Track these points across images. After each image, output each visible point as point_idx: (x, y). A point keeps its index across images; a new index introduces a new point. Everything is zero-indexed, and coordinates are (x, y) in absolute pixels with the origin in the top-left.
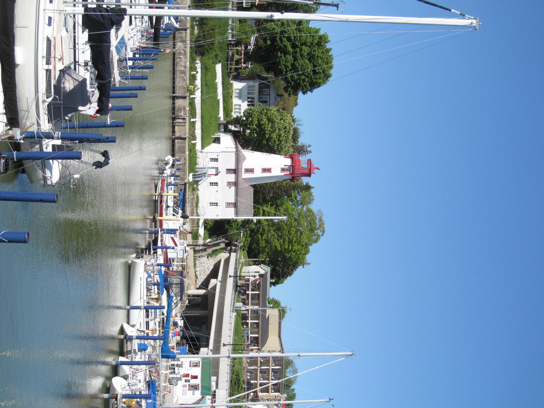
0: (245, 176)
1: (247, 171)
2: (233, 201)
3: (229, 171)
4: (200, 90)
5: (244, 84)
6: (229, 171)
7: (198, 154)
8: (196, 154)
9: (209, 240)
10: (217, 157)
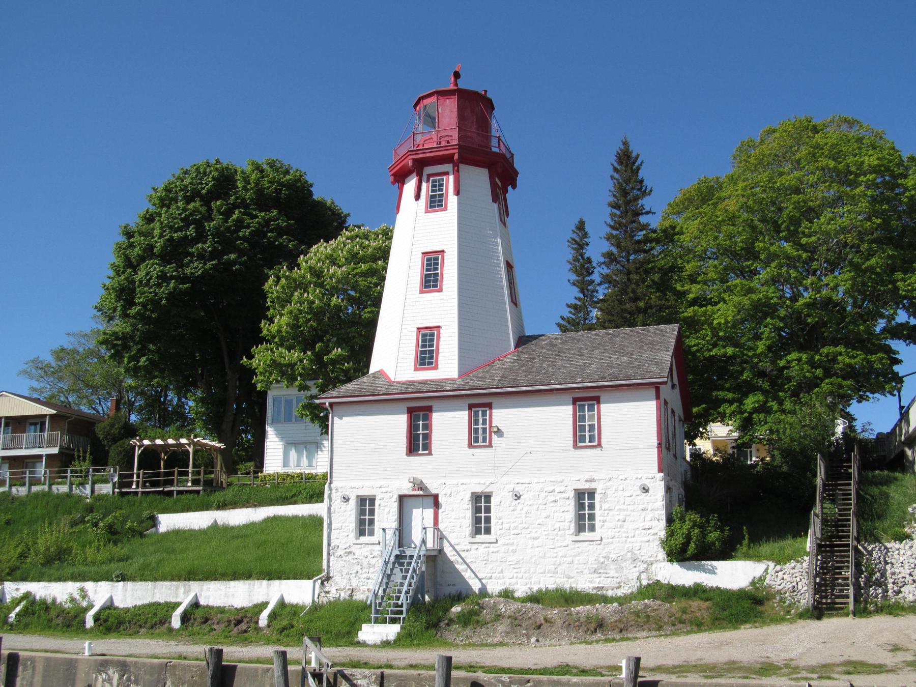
0: (448, 366)
2: (563, 414)
3: (418, 442)
4: (89, 586)
5: (270, 431)
6: (418, 442)
7: (333, 594)
8: (335, 605)
10: (353, 503)
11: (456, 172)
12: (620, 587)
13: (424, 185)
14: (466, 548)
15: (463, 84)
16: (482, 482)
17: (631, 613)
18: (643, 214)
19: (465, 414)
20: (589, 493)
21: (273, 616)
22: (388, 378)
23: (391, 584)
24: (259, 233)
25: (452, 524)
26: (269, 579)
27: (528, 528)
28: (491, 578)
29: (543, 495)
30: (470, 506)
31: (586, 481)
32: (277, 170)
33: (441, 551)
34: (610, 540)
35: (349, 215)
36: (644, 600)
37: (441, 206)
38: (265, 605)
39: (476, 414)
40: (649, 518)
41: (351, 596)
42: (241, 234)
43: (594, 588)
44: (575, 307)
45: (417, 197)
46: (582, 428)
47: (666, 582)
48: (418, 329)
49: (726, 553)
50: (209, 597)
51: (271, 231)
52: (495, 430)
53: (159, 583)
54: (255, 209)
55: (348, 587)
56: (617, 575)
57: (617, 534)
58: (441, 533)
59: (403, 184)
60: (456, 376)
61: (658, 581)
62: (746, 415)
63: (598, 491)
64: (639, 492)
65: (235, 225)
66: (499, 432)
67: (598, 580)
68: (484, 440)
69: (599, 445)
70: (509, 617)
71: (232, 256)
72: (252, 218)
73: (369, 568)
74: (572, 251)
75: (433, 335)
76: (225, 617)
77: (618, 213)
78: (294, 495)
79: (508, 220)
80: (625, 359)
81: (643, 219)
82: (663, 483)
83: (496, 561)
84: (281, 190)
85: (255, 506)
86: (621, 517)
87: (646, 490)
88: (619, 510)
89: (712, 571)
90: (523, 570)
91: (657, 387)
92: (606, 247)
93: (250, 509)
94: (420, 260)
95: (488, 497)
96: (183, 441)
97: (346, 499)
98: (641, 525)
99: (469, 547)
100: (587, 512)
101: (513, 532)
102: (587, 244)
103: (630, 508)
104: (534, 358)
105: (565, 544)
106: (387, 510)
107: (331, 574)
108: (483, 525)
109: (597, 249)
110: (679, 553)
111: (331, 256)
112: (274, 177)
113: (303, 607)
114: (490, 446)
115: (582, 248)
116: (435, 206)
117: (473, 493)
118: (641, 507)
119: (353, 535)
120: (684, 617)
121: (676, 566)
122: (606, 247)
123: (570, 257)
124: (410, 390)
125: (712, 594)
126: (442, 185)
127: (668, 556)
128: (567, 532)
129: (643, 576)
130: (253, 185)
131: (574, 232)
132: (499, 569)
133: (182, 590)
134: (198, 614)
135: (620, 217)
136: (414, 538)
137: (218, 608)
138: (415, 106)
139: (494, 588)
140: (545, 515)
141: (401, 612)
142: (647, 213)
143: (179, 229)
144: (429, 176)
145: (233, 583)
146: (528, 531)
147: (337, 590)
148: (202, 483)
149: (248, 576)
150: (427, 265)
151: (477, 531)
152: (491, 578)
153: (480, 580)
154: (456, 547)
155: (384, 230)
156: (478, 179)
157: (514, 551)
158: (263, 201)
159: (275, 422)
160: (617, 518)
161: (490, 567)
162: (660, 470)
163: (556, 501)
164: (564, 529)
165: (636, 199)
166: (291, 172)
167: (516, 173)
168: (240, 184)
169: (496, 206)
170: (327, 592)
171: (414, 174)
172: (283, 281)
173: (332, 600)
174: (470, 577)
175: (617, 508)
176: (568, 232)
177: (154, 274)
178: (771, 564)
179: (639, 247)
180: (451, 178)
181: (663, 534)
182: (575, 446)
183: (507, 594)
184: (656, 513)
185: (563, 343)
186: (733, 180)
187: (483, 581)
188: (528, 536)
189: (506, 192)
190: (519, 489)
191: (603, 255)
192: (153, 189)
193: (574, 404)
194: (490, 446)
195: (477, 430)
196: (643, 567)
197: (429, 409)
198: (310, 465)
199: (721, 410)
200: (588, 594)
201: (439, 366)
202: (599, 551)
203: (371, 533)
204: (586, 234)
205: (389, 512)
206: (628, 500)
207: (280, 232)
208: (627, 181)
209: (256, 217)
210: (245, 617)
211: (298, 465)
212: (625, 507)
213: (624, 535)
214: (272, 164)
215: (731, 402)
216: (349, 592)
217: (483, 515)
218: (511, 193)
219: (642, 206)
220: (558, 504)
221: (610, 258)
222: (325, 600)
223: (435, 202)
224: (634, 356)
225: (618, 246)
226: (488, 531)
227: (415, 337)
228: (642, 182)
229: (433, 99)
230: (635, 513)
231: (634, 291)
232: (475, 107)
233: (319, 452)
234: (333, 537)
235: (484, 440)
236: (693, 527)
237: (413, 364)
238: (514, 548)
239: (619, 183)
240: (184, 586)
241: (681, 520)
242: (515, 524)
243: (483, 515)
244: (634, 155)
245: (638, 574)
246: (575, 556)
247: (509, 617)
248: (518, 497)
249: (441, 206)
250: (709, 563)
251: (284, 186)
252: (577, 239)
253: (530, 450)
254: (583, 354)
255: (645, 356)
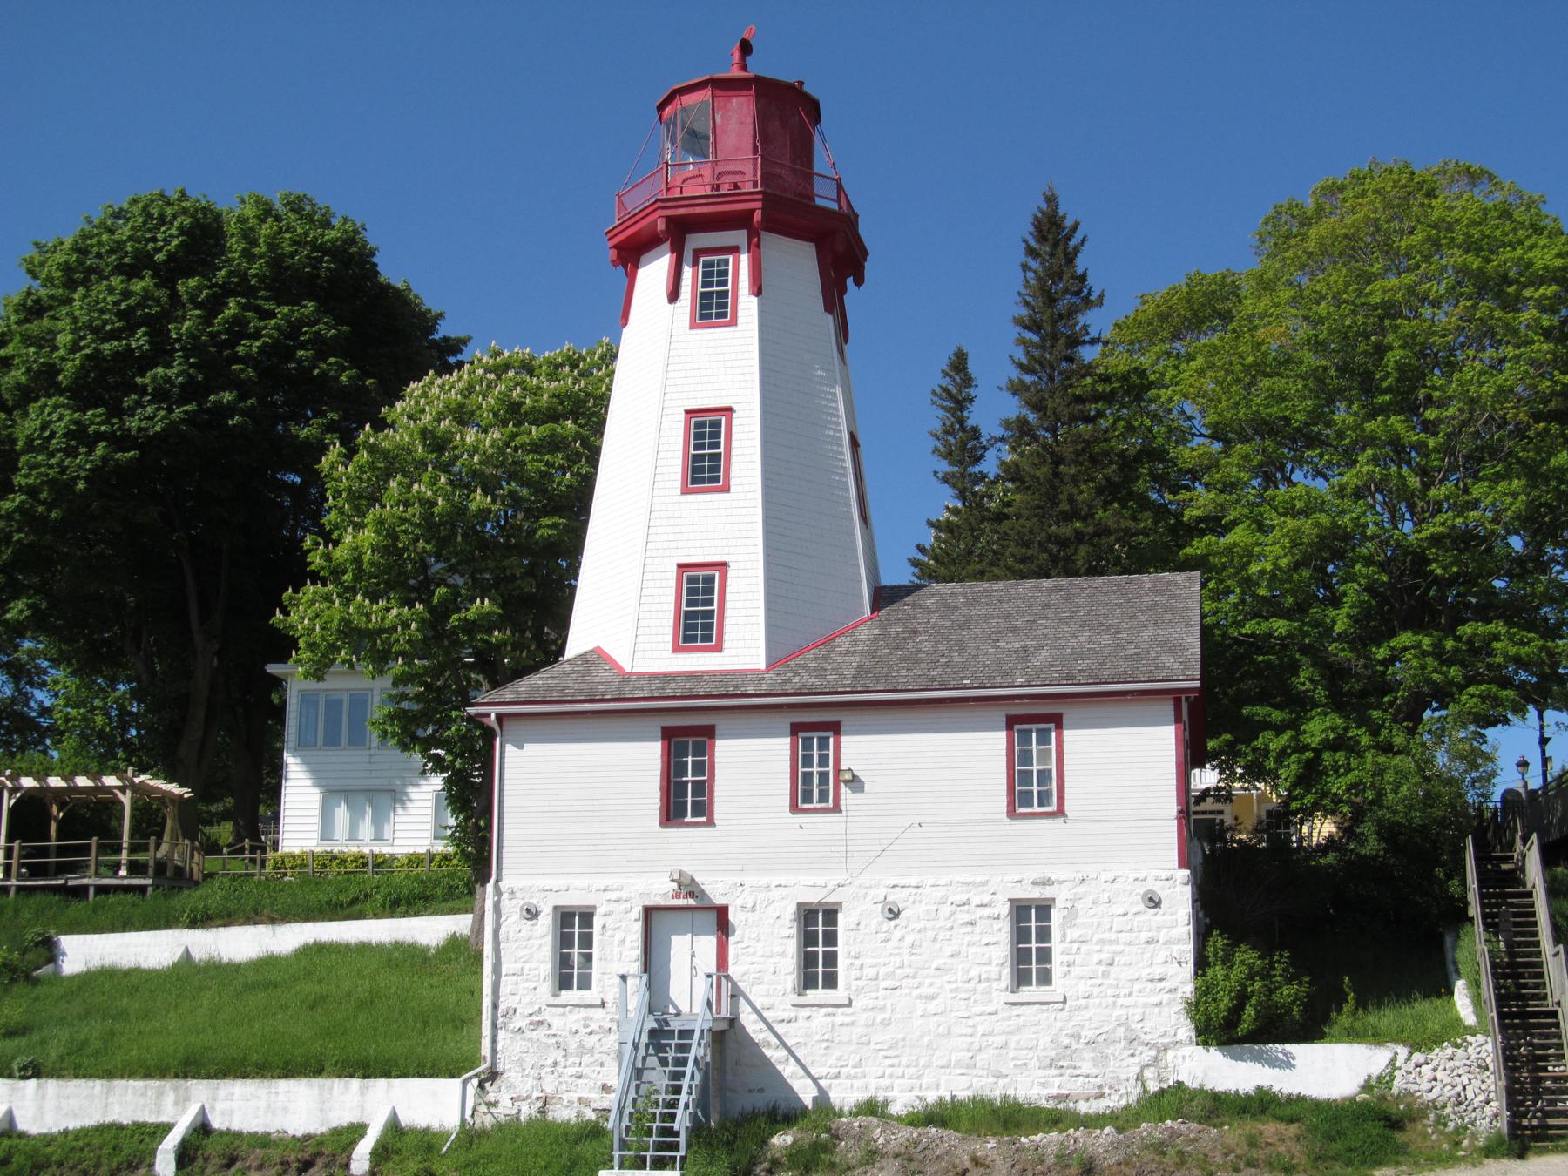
0: (744, 645)
1: (698, 619)
3: (684, 799)
5: (294, 766)
6: (684, 799)
7: (505, 1108)
8: (509, 1130)
9: (1462, 1002)
10: (546, 922)
11: (754, 247)
12: (1102, 1095)
13: (687, 272)
14: (786, 1015)
15: (758, 66)
16: (821, 881)
17: (1146, 1147)
18: (1084, 342)
19: (784, 743)
20: (1038, 908)
21: (381, 1153)
22: (615, 664)
23: (644, 1089)
24: (280, 351)
25: (758, 968)
26: (365, 1077)
27: (914, 977)
28: (837, 1076)
29: (946, 910)
30: (794, 931)
31: (1034, 883)
32: (310, 218)
33: (733, 1021)
34: (1083, 1002)
35: (441, 316)
36: (1162, 1120)
37: (724, 315)
38: (358, 1130)
39: (807, 744)
40: (1160, 958)
41: (543, 1111)
42: (241, 350)
43: (1049, 1098)
44: (948, 527)
45: (673, 296)
46: (1026, 777)
47: (1195, 1085)
48: (680, 566)
49: (1311, 1031)
50: (231, 1112)
51: (303, 346)
52: (848, 776)
53: (119, 1084)
54: (267, 299)
55: (536, 1094)
56: (1095, 1071)
57: (1096, 991)
58: (734, 984)
59: (636, 266)
60: (763, 666)
61: (1180, 1083)
62: (1309, 754)
63: (1059, 904)
64: (1141, 907)
65: (227, 331)
66: (855, 783)
67: (1057, 1081)
68: (823, 796)
69: (1061, 812)
70: (896, 1156)
71: (227, 397)
72: (262, 319)
73: (581, 1055)
74: (941, 413)
75: (711, 579)
76: (275, 1154)
77: (1035, 338)
78: (354, 901)
79: (846, 347)
80: (1106, 639)
81: (1088, 354)
82: (1189, 888)
83: (849, 1042)
84: (320, 260)
85: (272, 921)
86: (1105, 956)
87: (1154, 902)
88: (1102, 941)
89: (1287, 1063)
90: (904, 1060)
91: (1176, 696)
92: (1013, 408)
93: (261, 928)
94: (682, 425)
95: (831, 914)
96: (110, 781)
97: (532, 914)
98: (1145, 973)
99: (793, 1015)
100: (1034, 945)
101: (883, 984)
102: (972, 400)
103: (1123, 937)
104: (916, 632)
105: (991, 1009)
106: (619, 936)
107: (500, 1068)
108: (820, 969)
109: (994, 409)
110: (1221, 1027)
111: (461, 406)
112: (306, 234)
113: (444, 1135)
114: (836, 809)
115: (961, 408)
116: (710, 316)
117: (799, 905)
118: (1144, 936)
119: (546, 987)
120: (1254, 1153)
121: (1215, 1056)
122: (1013, 408)
123: (937, 426)
124: (669, 692)
125: (1295, 1108)
126: (726, 273)
127: (1199, 1033)
128: (995, 985)
129: (1149, 1074)
130: (264, 249)
131: (946, 374)
132: (854, 1059)
133: (170, 1098)
134: (213, 1148)
135: (1042, 347)
136: (673, 994)
137: (254, 1135)
138: (661, 107)
139: (845, 1096)
140: (949, 951)
141: (676, 1147)
142: (1093, 342)
143: (114, 335)
144: (697, 253)
145: (283, 1085)
146: (916, 982)
147: (512, 1099)
148: (151, 871)
149: (315, 1069)
150: (697, 436)
151: (808, 982)
152: (837, 1076)
153: (815, 1080)
154: (766, 1014)
155: (569, 358)
156: (797, 261)
157: (886, 1023)
158: (286, 281)
159: (302, 746)
160: (1096, 957)
161: (837, 1054)
162: (1182, 865)
163: (972, 924)
164: (988, 980)
165: (1072, 312)
166: (336, 222)
167: (865, 253)
168: (235, 245)
169: (830, 318)
170: (494, 1104)
171: (667, 245)
172: (364, 456)
173: (502, 1119)
174: (793, 1075)
175: (1096, 937)
176: (935, 377)
177: (60, 427)
178: (1402, 1051)
179: (1080, 408)
180: (744, 259)
181: (1188, 989)
182: (1012, 813)
183: (872, 1108)
184: (1175, 948)
185: (968, 603)
186: (1266, 285)
187: (822, 1082)
188: (915, 993)
189: (843, 290)
190: (896, 897)
191: (1007, 424)
192: (37, 245)
193: (1009, 727)
194: (836, 809)
195: (808, 777)
196: (1148, 1055)
197: (709, 732)
198: (378, 837)
199: (1259, 743)
200: (1039, 1111)
201: (726, 645)
202: (1059, 1024)
203: (585, 984)
204: (970, 379)
205: (623, 941)
206: (1118, 923)
207: (322, 348)
208: (1057, 276)
209: (272, 315)
210: (319, 1154)
211: (353, 836)
212: (1113, 936)
213: (1111, 992)
214: (295, 205)
215: (1279, 729)
216: (539, 1104)
217: (820, 949)
218: (853, 296)
219: (1085, 327)
220: (978, 929)
221: (1021, 430)
222: (488, 1121)
223: (710, 306)
224: (1124, 635)
225: (1038, 407)
226: (831, 981)
227: (673, 583)
228: (1083, 278)
229: (704, 95)
230: (1134, 949)
231: (1071, 500)
232: (787, 113)
233: (400, 811)
234: (503, 991)
235: (823, 796)
236: (1251, 977)
237: (670, 638)
238: (886, 1015)
239: (1039, 278)
240: (176, 1089)
241: (1224, 963)
242: (889, 969)
243: (820, 949)
244: (1068, 223)
245: (1137, 1069)
246: (1011, 1033)
247: (896, 1156)
248: (894, 914)
249: (724, 315)
250: (1279, 1047)
251: (325, 252)
252: (951, 388)
253: (919, 820)
254: (1015, 629)
255: (1145, 635)
